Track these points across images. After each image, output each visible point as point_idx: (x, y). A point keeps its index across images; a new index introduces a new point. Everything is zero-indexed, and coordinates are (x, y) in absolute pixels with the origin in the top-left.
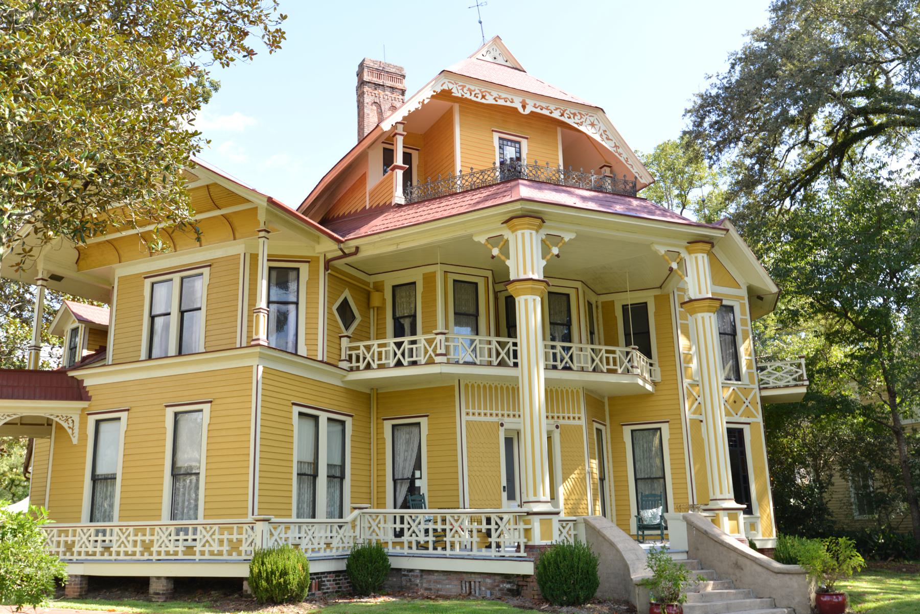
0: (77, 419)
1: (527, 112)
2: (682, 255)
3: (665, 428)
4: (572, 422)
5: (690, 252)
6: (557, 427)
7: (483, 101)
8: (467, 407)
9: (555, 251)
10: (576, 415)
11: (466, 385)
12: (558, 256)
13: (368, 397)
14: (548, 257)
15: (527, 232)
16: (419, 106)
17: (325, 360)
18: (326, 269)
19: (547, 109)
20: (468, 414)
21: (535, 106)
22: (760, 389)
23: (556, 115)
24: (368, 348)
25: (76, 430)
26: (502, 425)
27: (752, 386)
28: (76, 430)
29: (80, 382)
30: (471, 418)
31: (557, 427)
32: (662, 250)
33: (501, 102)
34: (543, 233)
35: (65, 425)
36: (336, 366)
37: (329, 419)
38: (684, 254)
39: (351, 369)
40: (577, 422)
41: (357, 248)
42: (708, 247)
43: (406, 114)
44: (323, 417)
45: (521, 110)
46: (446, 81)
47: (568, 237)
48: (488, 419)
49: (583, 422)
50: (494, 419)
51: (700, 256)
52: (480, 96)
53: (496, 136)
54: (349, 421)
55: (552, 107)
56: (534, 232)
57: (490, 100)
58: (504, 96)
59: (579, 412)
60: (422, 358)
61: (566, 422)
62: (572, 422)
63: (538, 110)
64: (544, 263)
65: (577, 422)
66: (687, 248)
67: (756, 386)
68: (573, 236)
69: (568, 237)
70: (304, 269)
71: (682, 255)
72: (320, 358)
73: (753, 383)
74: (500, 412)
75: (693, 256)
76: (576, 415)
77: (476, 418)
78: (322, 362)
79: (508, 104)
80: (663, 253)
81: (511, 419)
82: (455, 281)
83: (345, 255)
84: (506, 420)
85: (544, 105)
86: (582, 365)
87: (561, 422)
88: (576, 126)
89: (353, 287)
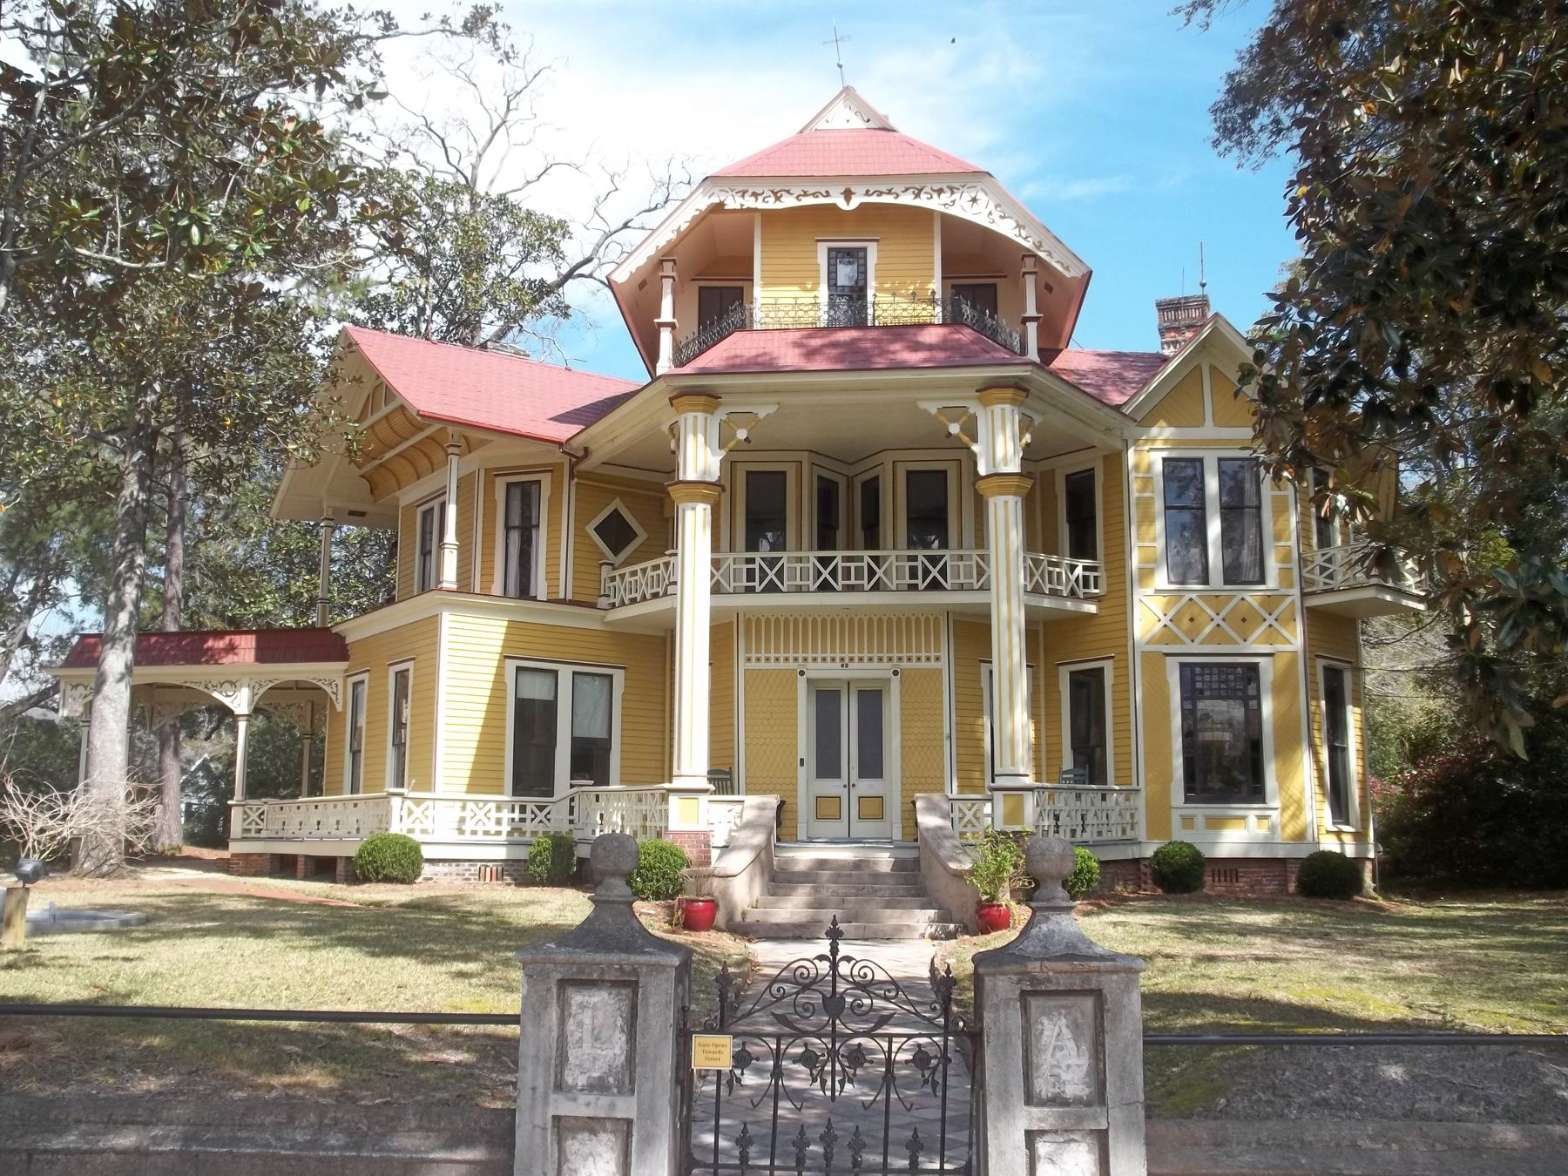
0: (340, 682)
1: (855, 202)
2: (971, 411)
3: (1108, 667)
4: (924, 664)
5: (985, 404)
6: (896, 673)
7: (779, 206)
8: (748, 650)
9: (742, 434)
10: (932, 655)
11: (748, 621)
12: (747, 440)
13: (664, 638)
14: (731, 445)
15: (690, 416)
16: (673, 236)
17: (569, 597)
18: (572, 476)
19: (889, 192)
20: (749, 660)
21: (867, 193)
22: (1304, 595)
23: (907, 199)
24: (622, 576)
25: (340, 696)
26: (802, 673)
27: (1283, 591)
28: (340, 696)
29: (340, 638)
30: (753, 665)
31: (896, 673)
32: (933, 408)
33: (808, 201)
34: (721, 414)
35: (329, 690)
36: (593, 606)
37: (574, 673)
38: (974, 408)
39: (613, 606)
40: (933, 664)
41: (586, 449)
42: (1009, 393)
43: (653, 252)
44: (565, 673)
45: (842, 204)
46: (716, 190)
47: (762, 413)
48: (782, 665)
49: (943, 664)
50: (791, 665)
51: (997, 408)
52: (772, 199)
53: (822, 249)
54: (619, 677)
55: (898, 189)
56: (701, 416)
57: (789, 202)
58: (811, 191)
59: (937, 649)
60: (810, 582)
61: (914, 665)
62: (924, 664)
63: (874, 199)
64: (723, 453)
65: (933, 664)
66: (979, 398)
67: (1296, 591)
68: (772, 409)
69: (762, 413)
70: (546, 480)
71: (971, 411)
72: (562, 596)
73: (1291, 586)
74: (800, 655)
75: (989, 409)
76: (932, 655)
77: (763, 665)
78: (563, 602)
79: (821, 200)
80: (933, 411)
81: (819, 664)
82: (748, 473)
83: (580, 460)
84: (810, 664)
85: (884, 189)
86: (962, 580)
87: (905, 665)
88: (942, 209)
89: (622, 495)
